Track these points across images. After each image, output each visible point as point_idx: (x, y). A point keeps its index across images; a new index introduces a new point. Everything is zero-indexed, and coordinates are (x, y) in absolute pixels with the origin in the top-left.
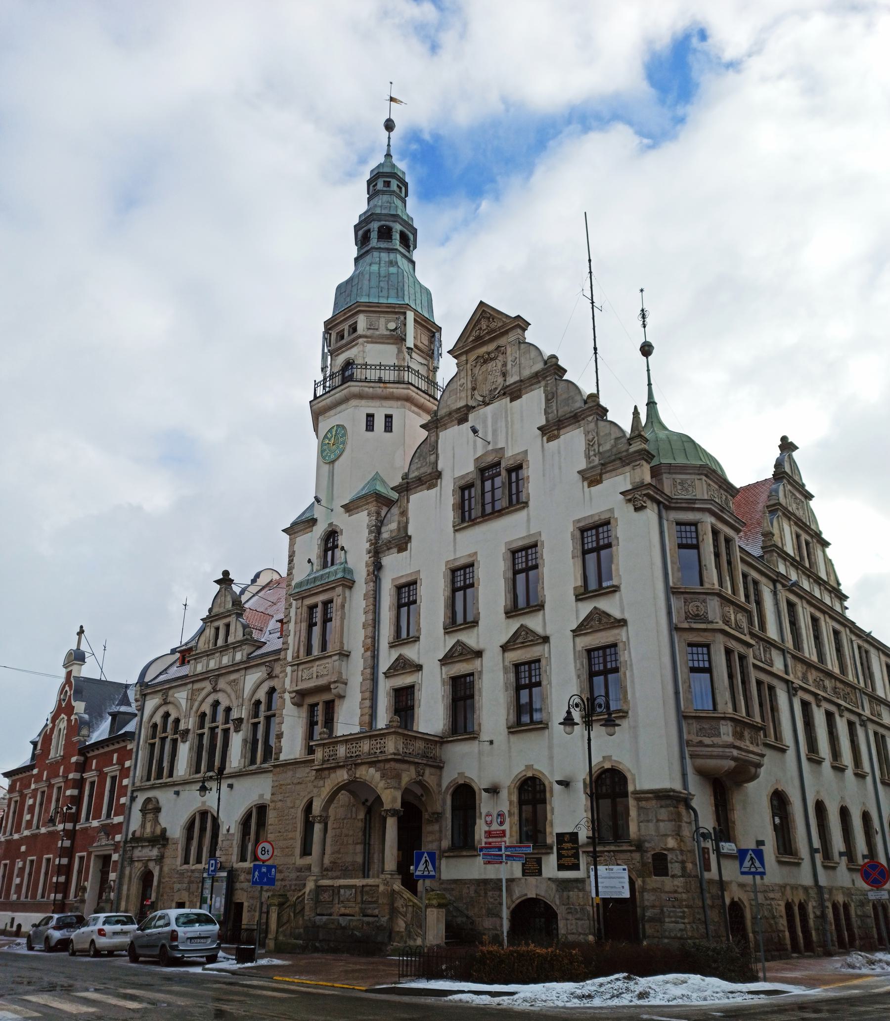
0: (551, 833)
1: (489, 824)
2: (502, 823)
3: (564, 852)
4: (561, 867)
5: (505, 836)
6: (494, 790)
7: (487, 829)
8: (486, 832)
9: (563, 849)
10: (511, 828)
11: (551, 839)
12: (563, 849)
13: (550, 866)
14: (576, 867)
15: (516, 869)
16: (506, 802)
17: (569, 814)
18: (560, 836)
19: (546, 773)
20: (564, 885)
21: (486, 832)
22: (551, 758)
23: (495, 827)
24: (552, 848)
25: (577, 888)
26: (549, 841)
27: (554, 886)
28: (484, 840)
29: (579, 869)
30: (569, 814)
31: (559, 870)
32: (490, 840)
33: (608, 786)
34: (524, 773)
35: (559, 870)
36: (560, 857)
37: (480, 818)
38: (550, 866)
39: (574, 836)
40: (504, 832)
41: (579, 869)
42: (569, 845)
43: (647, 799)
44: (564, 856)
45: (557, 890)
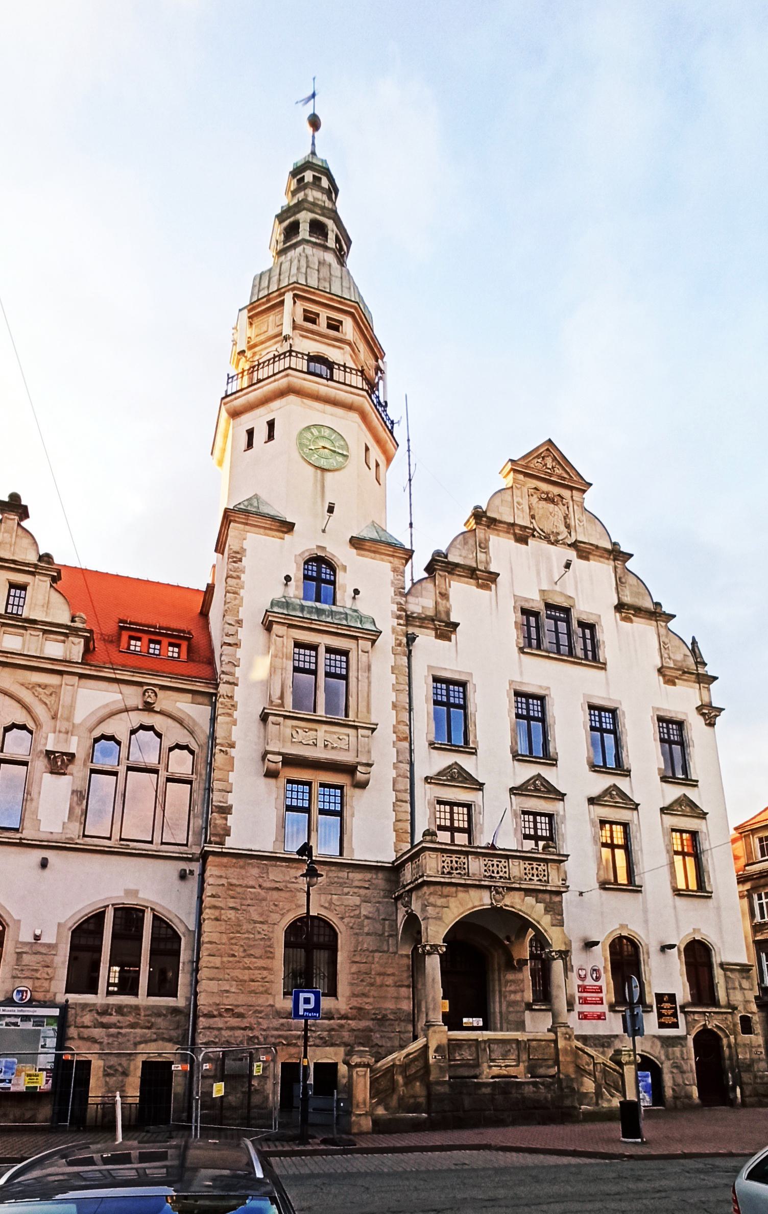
0: (650, 992)
1: (583, 979)
2: (597, 979)
3: (663, 1011)
4: (662, 1025)
5: (601, 992)
6: (589, 945)
7: (580, 983)
8: (579, 986)
9: (663, 1008)
10: (608, 984)
11: (651, 999)
12: (663, 1008)
13: (650, 1023)
14: (675, 1025)
15: (614, 1025)
16: (601, 958)
17: (666, 976)
18: (660, 997)
19: (643, 936)
20: (667, 1042)
21: (579, 986)
22: (646, 922)
23: (589, 982)
24: (651, 1007)
25: (681, 1044)
26: (648, 1001)
27: (658, 1043)
28: (577, 995)
29: (678, 1027)
30: (666, 976)
31: (660, 1027)
32: (585, 995)
33: (698, 956)
34: (619, 932)
35: (660, 1027)
36: (660, 1015)
37: (572, 971)
38: (650, 1023)
39: (672, 998)
40: (600, 988)
41: (678, 1027)
42: (668, 1005)
43: (732, 970)
44: (663, 1015)
45: (662, 1046)
